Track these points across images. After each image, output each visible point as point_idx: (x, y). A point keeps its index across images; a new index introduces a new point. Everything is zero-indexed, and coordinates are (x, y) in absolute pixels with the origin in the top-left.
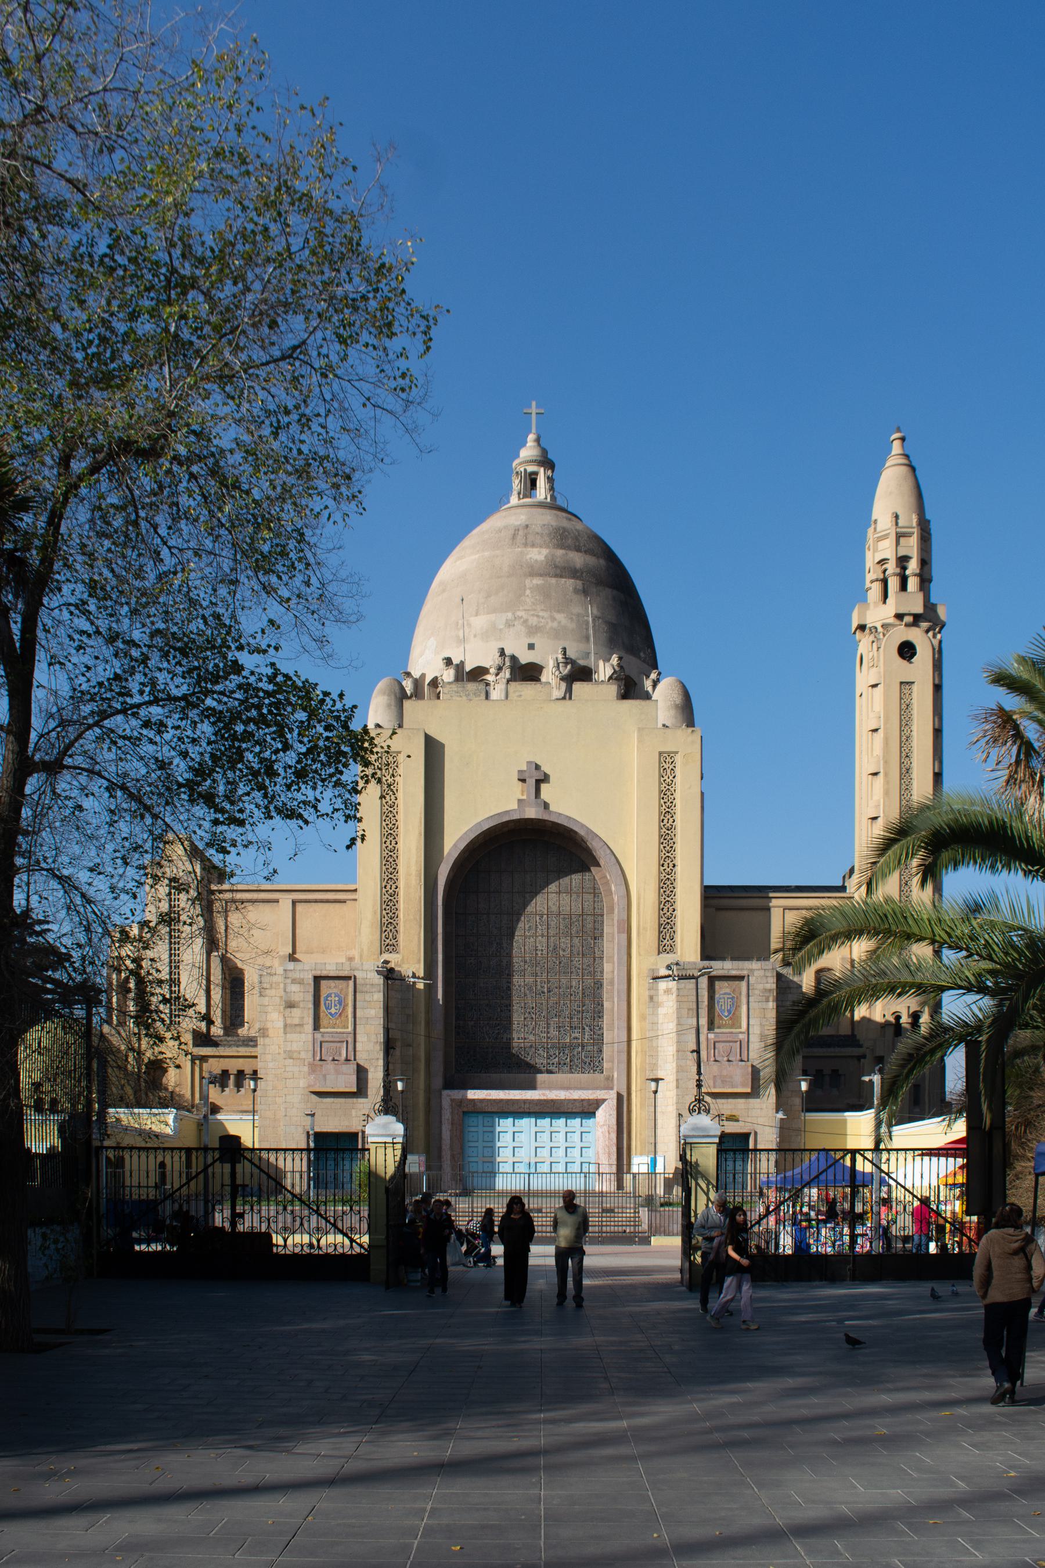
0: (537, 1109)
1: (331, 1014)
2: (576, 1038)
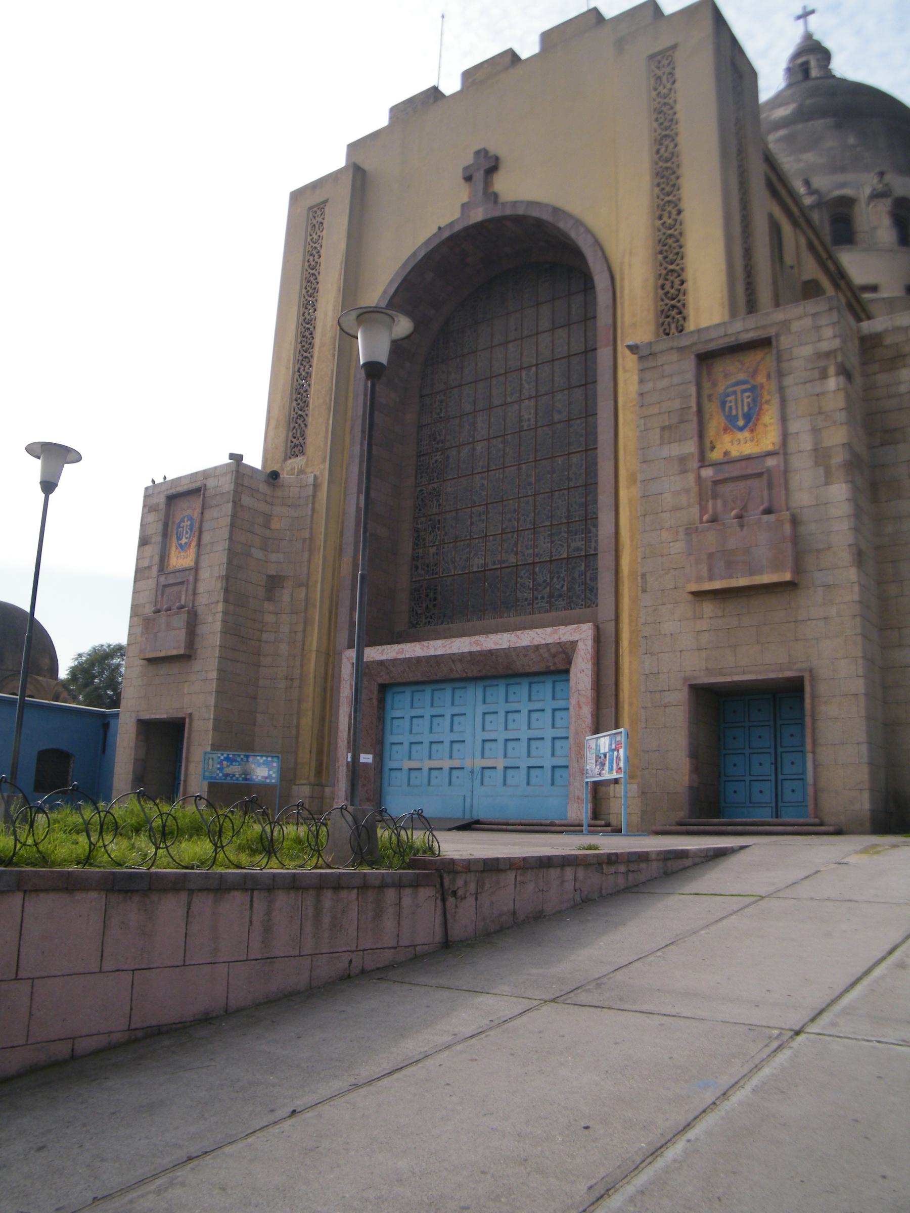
0: (474, 672)
1: (181, 545)
2: (578, 549)
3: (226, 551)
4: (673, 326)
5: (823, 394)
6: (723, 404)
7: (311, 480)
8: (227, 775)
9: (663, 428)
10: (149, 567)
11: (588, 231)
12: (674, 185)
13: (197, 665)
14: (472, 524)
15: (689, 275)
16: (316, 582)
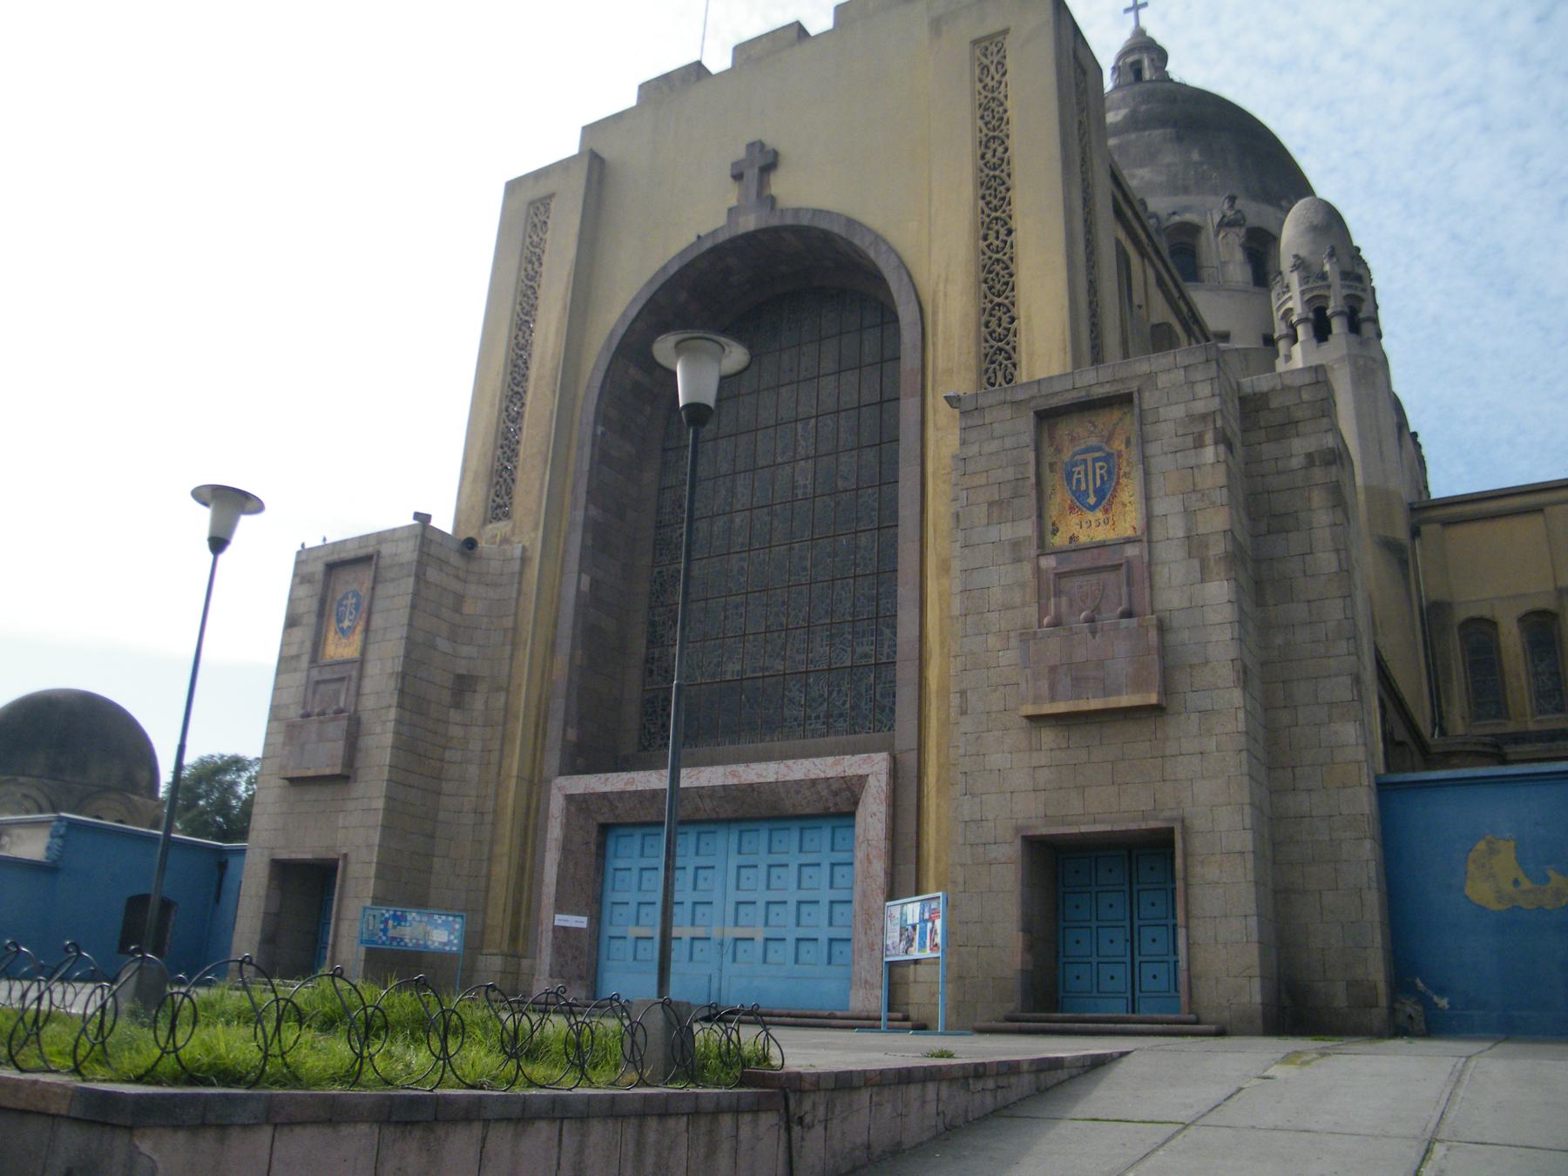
0: (727, 811)
1: (342, 630)
2: (866, 656)
3: (403, 641)
4: (1000, 374)
5: (1198, 466)
6: (1069, 476)
7: (518, 552)
8: (393, 939)
9: (991, 504)
10: (297, 657)
11: (892, 250)
12: (1003, 199)
13: (358, 789)
14: (726, 618)
15: (1021, 311)
16: (520, 685)
